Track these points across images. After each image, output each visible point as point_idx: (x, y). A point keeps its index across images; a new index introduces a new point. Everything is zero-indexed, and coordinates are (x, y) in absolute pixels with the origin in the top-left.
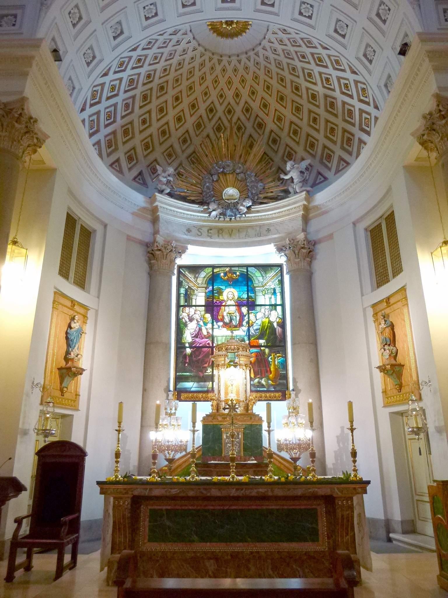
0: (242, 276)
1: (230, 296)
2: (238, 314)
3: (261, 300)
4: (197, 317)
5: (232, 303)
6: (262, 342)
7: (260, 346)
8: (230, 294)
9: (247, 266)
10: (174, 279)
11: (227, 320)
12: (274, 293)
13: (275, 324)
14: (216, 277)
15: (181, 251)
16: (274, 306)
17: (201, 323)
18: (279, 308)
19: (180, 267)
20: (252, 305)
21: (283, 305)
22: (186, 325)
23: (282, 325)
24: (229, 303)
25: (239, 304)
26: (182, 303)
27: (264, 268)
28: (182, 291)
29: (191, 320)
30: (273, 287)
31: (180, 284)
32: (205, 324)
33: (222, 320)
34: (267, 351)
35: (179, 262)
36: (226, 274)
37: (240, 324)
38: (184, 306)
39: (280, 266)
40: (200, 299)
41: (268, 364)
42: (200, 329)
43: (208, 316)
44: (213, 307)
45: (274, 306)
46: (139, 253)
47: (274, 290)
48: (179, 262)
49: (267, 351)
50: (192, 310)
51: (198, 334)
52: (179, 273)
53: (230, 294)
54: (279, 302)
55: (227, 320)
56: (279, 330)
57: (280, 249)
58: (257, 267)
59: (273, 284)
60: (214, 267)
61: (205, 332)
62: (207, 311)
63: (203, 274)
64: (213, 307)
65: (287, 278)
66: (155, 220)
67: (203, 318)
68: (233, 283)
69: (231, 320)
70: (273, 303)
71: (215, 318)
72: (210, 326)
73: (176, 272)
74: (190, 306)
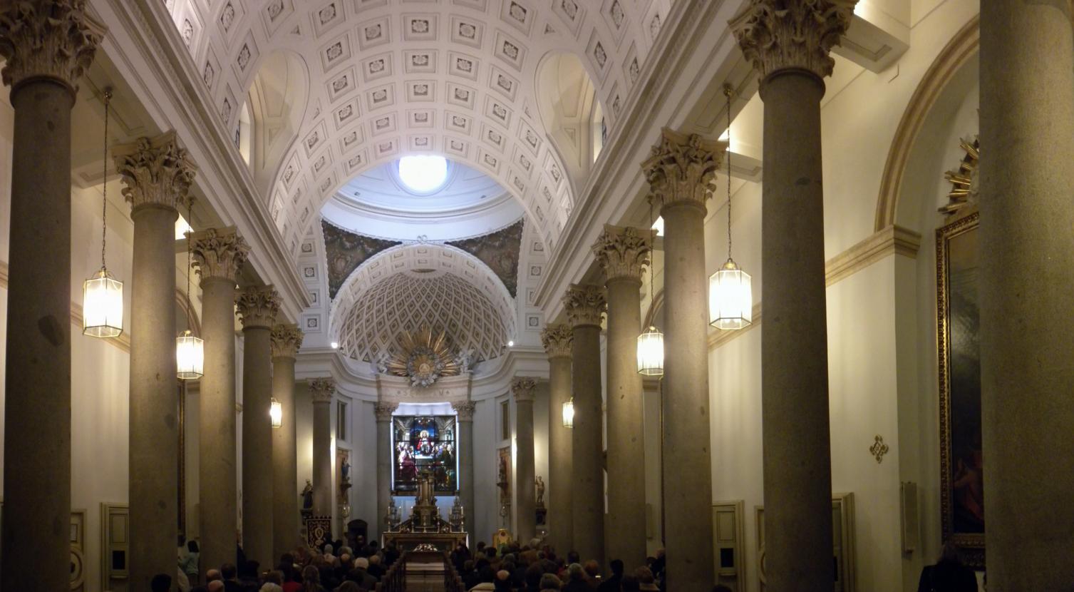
0: (433, 424)
1: (424, 435)
2: (429, 446)
3: (445, 438)
4: (406, 447)
5: (426, 439)
6: (442, 462)
7: (441, 465)
8: (424, 434)
9: (435, 417)
10: (392, 424)
11: (423, 450)
12: (450, 434)
13: (450, 453)
14: (415, 424)
15: (394, 409)
16: (449, 442)
17: (408, 451)
18: (452, 443)
19: (395, 417)
20: (437, 441)
21: (455, 441)
22: (399, 453)
23: (454, 452)
24: (424, 439)
25: (430, 440)
26: (397, 439)
27: (445, 418)
28: (397, 432)
29: (402, 449)
30: (449, 429)
31: (395, 428)
32: (410, 452)
33: (420, 449)
34: (445, 468)
35: (394, 414)
36: (422, 421)
37: (430, 452)
38: (398, 441)
39: (454, 417)
40: (407, 436)
41: (445, 475)
42: (408, 455)
43: (412, 447)
44: (414, 441)
45: (449, 442)
46: (371, 408)
47: (450, 431)
48: (394, 414)
49: (445, 468)
50: (402, 444)
51: (406, 458)
52: (394, 421)
53: (424, 434)
54: (452, 439)
55: (423, 450)
56: (452, 456)
57: (454, 407)
58: (441, 417)
59: (449, 428)
60: (414, 417)
61: (410, 457)
62: (411, 445)
63: (408, 421)
64: (414, 441)
65: (457, 425)
66: (379, 387)
67: (409, 448)
68: (426, 427)
69: (425, 450)
70: (449, 439)
71: (416, 449)
72: (413, 453)
73: (392, 420)
74: (402, 441)
